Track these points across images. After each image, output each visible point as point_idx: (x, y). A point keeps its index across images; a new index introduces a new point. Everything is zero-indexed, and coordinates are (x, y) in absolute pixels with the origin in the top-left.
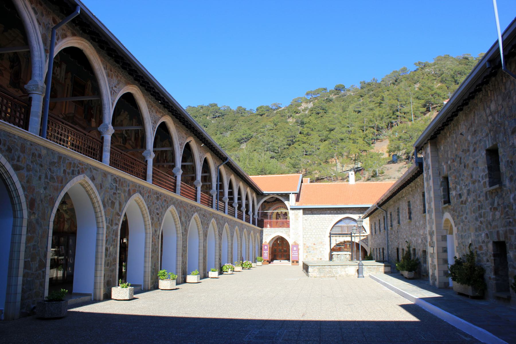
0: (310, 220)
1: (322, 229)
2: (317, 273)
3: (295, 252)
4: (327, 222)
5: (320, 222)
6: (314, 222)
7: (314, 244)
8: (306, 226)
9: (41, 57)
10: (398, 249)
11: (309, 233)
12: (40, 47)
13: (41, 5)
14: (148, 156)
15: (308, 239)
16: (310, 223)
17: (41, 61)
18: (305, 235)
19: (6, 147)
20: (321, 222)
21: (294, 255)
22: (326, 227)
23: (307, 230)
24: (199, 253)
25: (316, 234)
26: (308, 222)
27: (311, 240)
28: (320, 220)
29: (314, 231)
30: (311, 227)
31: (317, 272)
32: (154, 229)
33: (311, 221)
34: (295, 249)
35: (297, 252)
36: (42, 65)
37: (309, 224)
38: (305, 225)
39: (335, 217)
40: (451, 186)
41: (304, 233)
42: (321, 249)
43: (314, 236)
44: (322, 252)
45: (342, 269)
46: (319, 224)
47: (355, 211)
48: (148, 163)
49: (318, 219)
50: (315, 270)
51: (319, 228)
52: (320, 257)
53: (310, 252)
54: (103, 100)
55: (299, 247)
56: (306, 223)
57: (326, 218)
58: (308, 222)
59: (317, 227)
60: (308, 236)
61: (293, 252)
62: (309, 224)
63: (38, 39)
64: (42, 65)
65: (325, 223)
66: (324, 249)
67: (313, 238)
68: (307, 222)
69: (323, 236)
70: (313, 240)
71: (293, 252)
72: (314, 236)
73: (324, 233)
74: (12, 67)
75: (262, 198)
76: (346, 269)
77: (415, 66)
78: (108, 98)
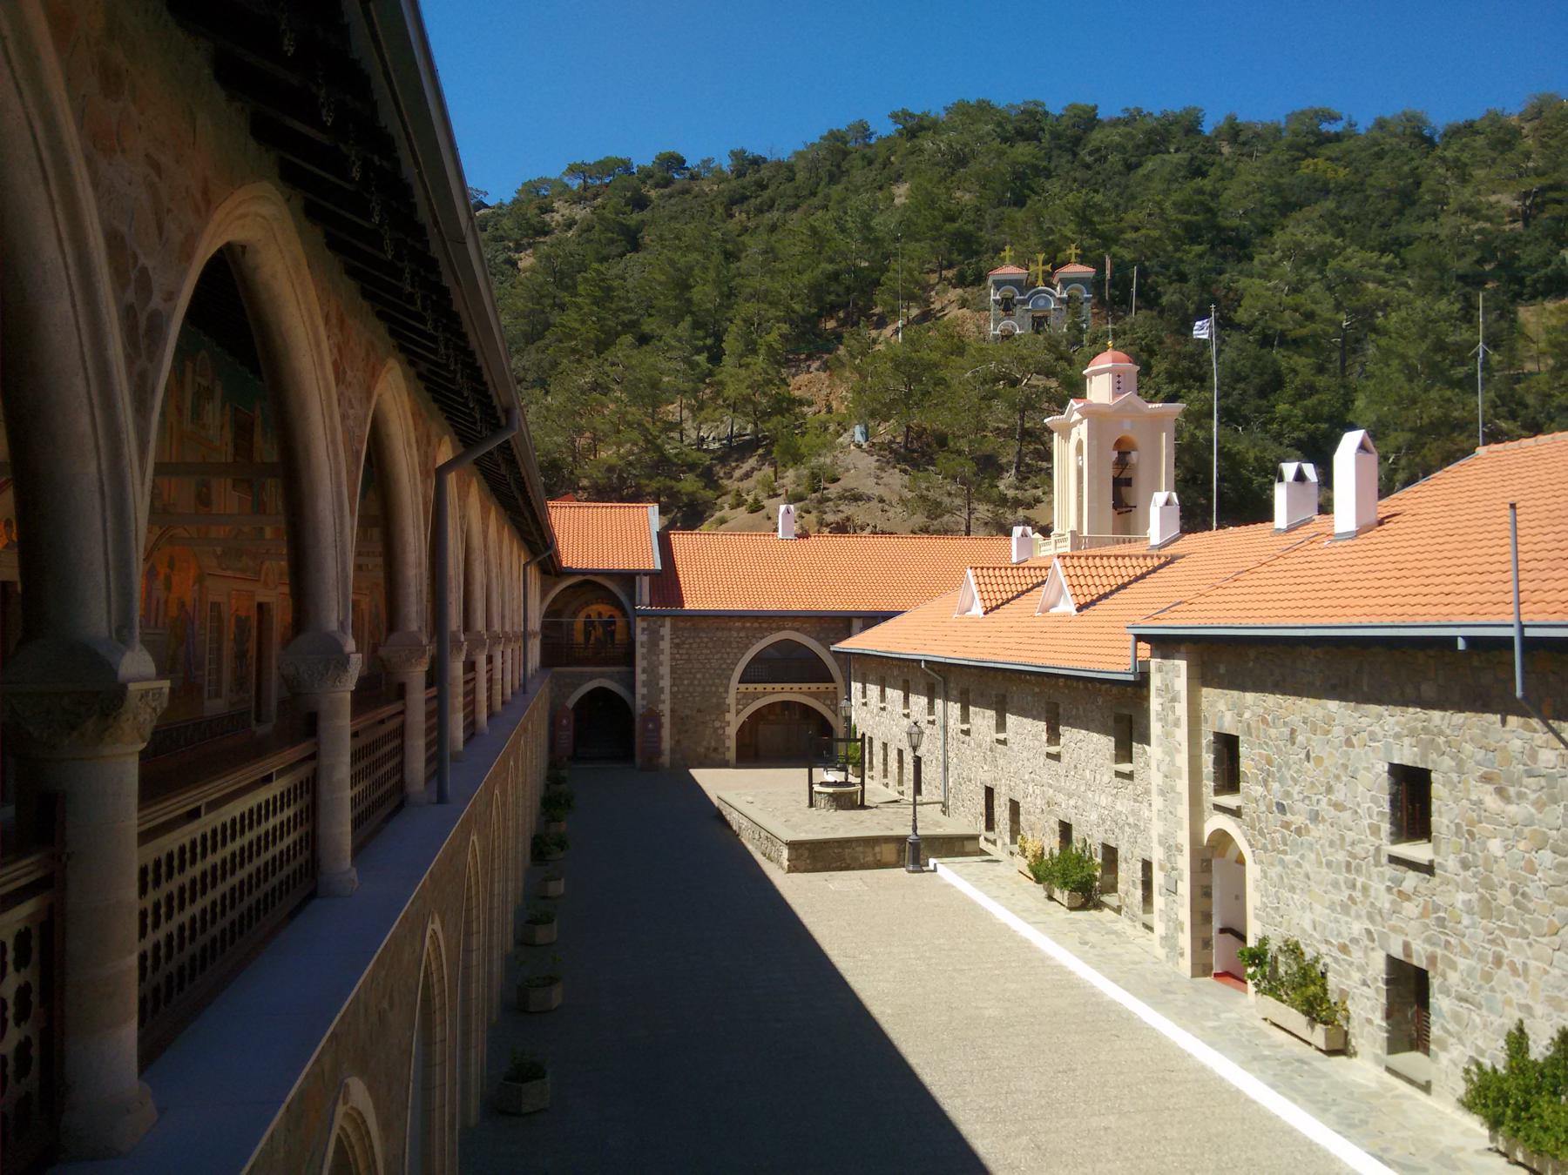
7: (699, 711)
10: (989, 792)
29: (699, 676)
40: (1245, 765)
42: (717, 724)
44: (720, 732)
49: (710, 645)
52: (713, 744)
53: (686, 731)
72: (699, 689)
75: (556, 584)
76: (877, 849)
77: (891, 121)
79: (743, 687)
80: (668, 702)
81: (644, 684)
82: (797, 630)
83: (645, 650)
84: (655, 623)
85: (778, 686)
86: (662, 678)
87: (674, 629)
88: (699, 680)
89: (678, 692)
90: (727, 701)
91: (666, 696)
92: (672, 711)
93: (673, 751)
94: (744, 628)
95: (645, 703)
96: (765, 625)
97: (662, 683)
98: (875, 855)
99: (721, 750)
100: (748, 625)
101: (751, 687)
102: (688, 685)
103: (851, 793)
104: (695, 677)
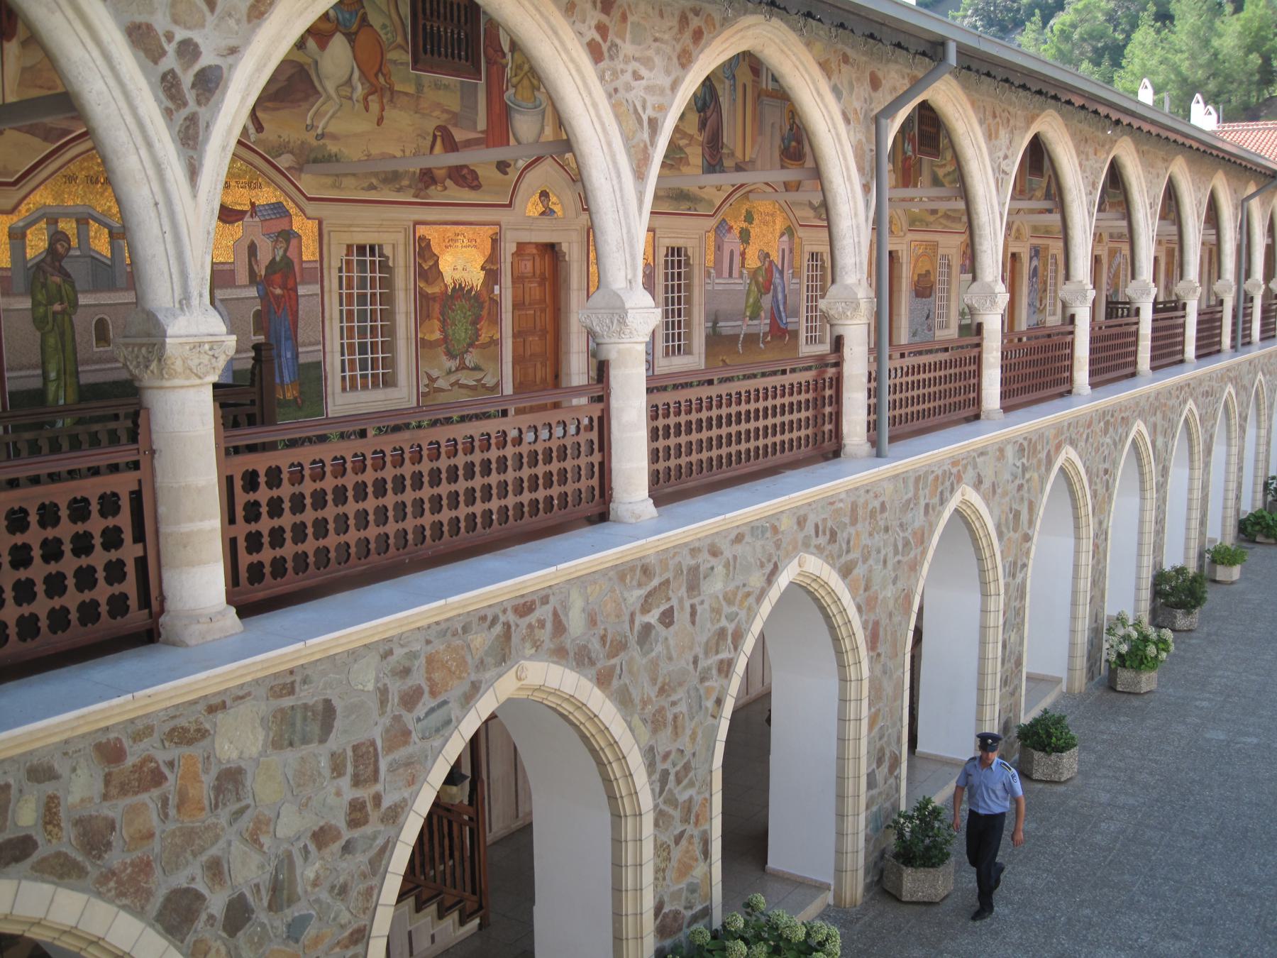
9: (856, 215)
12: (852, 190)
13: (846, 59)
14: (1078, 302)
17: (858, 227)
19: (828, 533)
24: (1189, 509)
32: (1096, 520)
36: (859, 236)
48: (1077, 321)
54: (977, 213)
63: (848, 169)
64: (859, 236)
74: (703, 125)
78: (992, 205)
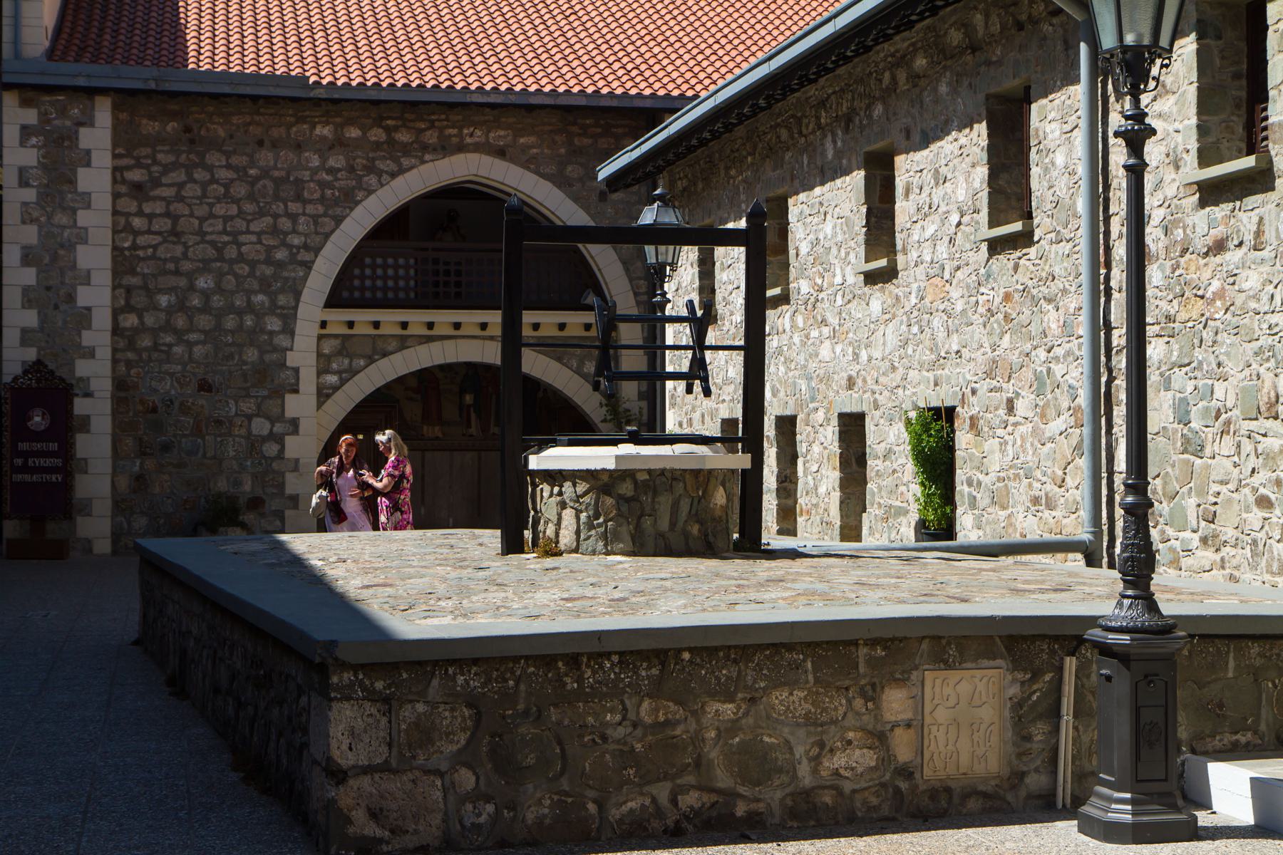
0: (168, 192)
1: (269, 271)
2: (466, 779)
3: (38, 446)
4: (310, 209)
5: (249, 207)
6: (201, 211)
7: (205, 387)
8: (141, 240)
11: (164, 300)
15: (156, 347)
16: (175, 218)
18: (129, 308)
20: (261, 214)
21: (25, 469)
22: (304, 256)
23: (144, 268)
25: (217, 301)
26: (159, 208)
27: (178, 350)
28: (251, 197)
29: (203, 282)
30: (179, 250)
31: (465, 758)
33: (180, 198)
34: (38, 420)
35: (54, 446)
37: (164, 224)
38: (129, 228)
39: (372, 180)
41: (121, 291)
42: (260, 426)
43: (204, 321)
44: (271, 449)
45: (838, 705)
46: (240, 224)
47: (532, 139)
49: (240, 190)
50: (424, 734)
51: (241, 258)
53: (166, 448)
55: (81, 406)
56: (140, 213)
57: (299, 182)
58: (159, 208)
59: (231, 252)
60: (149, 320)
61: (24, 446)
62: (164, 224)
65: (293, 217)
66: (278, 428)
67: (193, 337)
68: (147, 208)
69: (273, 324)
70: (198, 351)
71: (24, 446)
72: (204, 321)
73: (282, 300)
76: (895, 702)
79: (338, 317)
80: (104, 353)
81: (29, 296)
82: (501, 153)
83: (30, 195)
84: (63, 112)
85: (442, 318)
86: (87, 282)
87: (124, 141)
88: (206, 295)
89: (141, 329)
90: (292, 359)
91: (99, 336)
92: (120, 385)
93: (120, 505)
94: (339, 143)
95: (31, 354)
96: (403, 137)
97: (84, 296)
98: (879, 738)
99: (274, 504)
100: (354, 133)
101: (363, 317)
102: (170, 311)
103: (702, 478)
104: (192, 288)
